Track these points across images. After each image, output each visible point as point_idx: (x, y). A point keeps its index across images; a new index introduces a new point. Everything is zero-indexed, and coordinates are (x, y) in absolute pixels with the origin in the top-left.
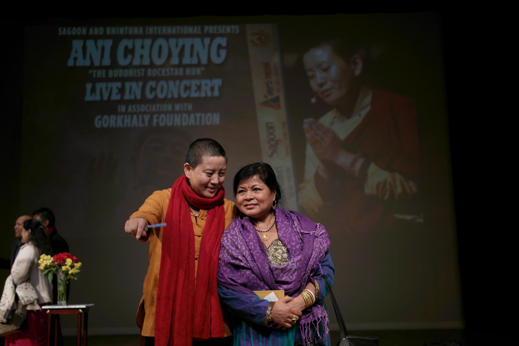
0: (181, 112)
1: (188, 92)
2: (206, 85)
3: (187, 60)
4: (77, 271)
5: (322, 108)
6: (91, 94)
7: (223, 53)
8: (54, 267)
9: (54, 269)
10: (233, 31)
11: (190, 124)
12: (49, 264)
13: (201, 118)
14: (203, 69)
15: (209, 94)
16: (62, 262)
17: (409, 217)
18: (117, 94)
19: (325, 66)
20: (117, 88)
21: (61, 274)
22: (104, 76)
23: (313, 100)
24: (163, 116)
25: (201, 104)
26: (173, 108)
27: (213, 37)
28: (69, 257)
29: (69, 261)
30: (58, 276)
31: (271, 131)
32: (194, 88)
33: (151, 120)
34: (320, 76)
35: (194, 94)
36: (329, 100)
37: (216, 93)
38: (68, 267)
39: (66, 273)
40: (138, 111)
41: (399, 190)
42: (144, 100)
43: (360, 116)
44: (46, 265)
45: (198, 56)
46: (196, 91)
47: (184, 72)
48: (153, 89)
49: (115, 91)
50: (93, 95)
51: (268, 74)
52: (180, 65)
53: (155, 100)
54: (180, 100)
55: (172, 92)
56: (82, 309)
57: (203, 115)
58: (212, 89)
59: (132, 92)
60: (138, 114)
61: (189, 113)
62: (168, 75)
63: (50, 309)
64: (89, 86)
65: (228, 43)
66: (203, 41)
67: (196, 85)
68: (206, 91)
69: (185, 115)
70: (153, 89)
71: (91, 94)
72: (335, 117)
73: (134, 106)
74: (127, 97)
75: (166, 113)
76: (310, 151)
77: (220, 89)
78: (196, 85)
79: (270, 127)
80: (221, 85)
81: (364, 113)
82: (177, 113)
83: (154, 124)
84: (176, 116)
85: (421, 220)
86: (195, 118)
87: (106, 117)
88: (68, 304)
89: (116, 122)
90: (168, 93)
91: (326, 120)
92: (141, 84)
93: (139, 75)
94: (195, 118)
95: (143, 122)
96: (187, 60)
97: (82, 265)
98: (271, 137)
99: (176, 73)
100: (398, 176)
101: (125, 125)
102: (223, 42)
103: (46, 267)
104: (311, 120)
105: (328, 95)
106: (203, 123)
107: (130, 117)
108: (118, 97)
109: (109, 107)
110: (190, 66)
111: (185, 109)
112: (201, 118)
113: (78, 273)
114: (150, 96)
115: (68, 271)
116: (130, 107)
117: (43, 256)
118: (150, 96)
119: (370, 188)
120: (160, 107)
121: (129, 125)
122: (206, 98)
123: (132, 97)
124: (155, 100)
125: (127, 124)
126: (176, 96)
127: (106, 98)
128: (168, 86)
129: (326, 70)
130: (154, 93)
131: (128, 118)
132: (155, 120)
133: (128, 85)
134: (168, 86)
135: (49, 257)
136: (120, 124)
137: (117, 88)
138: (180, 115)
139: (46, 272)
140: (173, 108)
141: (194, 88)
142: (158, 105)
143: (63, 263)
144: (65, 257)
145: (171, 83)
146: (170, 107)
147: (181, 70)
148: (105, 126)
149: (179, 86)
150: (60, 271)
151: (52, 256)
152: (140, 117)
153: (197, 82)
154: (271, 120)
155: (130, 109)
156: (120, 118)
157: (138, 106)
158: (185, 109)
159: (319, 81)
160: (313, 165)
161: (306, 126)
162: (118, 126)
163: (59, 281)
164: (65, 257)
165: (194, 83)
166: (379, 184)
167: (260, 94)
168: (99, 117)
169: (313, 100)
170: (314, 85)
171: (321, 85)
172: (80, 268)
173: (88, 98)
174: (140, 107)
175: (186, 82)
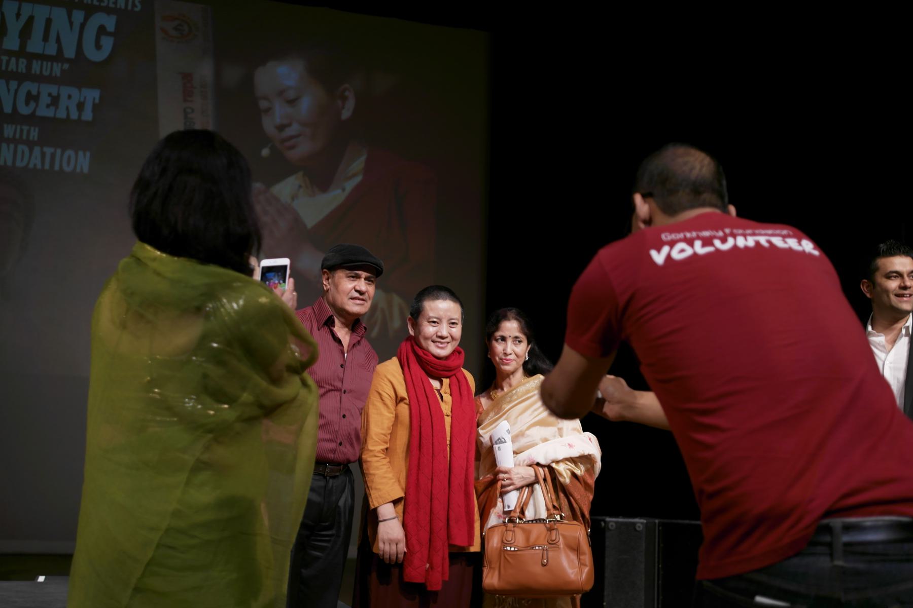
1: (32, 105)
2: (70, 97)
3: (35, 45)
7: (108, 43)
10: (130, 7)
11: (31, 166)
13: (53, 156)
14: (66, 66)
15: (74, 115)
19: (291, 94)
23: (265, 152)
25: (55, 132)
27: (90, 11)
32: (45, 100)
34: (280, 112)
35: (43, 111)
36: (293, 155)
37: (88, 115)
43: (344, 190)
45: (58, 40)
46: (48, 106)
47: (29, 67)
51: (187, 94)
52: (22, 53)
57: (59, 151)
58: (80, 106)
61: (31, 145)
65: (118, 25)
66: (70, 16)
67: (50, 95)
68: (67, 108)
69: (21, 147)
72: (300, 187)
77: (95, 106)
78: (50, 95)
80: (97, 101)
81: (350, 186)
86: (43, 155)
91: (285, 189)
94: (43, 155)
96: (35, 45)
99: (12, 66)
100: (397, 300)
102: (110, 23)
105: (292, 147)
106: (57, 168)
110: (42, 57)
111: (24, 137)
112: (53, 156)
129: (292, 102)
138: (12, 146)
141: (45, 100)
147: (23, 62)
149: (16, 91)
158: (24, 137)
159: (278, 121)
165: (47, 90)
169: (265, 152)
170: (269, 124)
171: (281, 128)
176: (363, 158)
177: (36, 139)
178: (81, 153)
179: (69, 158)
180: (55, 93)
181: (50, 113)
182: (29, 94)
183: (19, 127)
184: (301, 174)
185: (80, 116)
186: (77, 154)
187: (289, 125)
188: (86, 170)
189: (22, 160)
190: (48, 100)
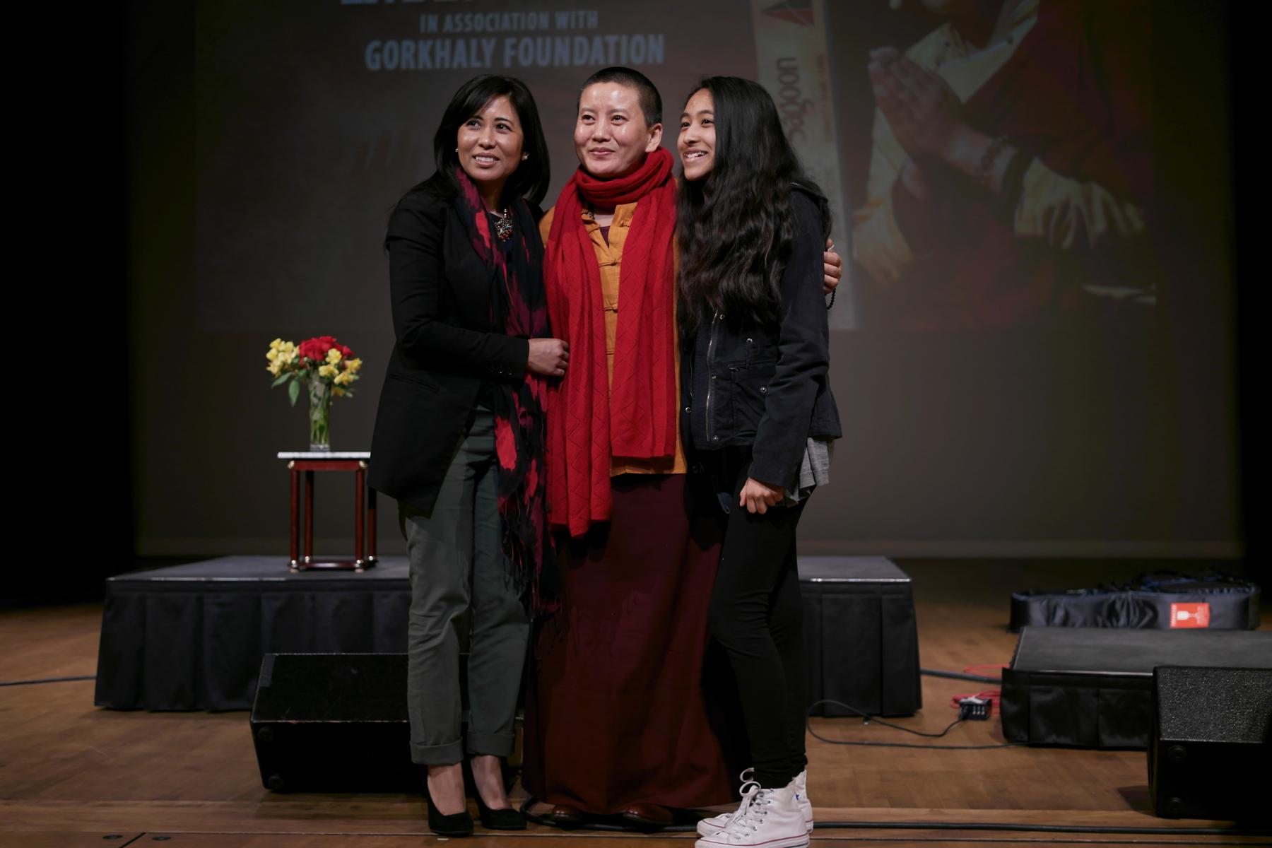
0: (571, 32)
4: (352, 377)
5: (916, 23)
8: (302, 367)
9: (302, 373)
11: (592, 62)
12: (289, 361)
13: (618, 45)
16: (318, 357)
17: (1120, 293)
21: (316, 383)
24: (527, 41)
26: (552, 21)
28: (333, 346)
29: (334, 355)
30: (311, 388)
33: (499, 50)
38: (331, 367)
39: (328, 382)
40: (468, 29)
41: (1100, 226)
43: (1010, 41)
44: (284, 364)
56: (365, 460)
57: (624, 38)
60: (466, 36)
61: (589, 34)
69: (580, 40)
72: (947, 45)
73: (458, 17)
75: (534, 34)
76: (882, 128)
79: (786, 70)
81: (1019, 34)
83: (507, 63)
84: (558, 40)
85: (1152, 300)
86: (606, 46)
87: (392, 44)
88: (332, 450)
89: (416, 56)
91: (925, 51)
94: (606, 46)
95: (480, 56)
97: (362, 366)
98: (789, 93)
100: (1098, 192)
101: (438, 65)
103: (284, 369)
104: (888, 50)
107: (448, 43)
111: (581, 25)
112: (618, 45)
113: (355, 381)
115: (332, 376)
116: (448, 18)
117: (276, 344)
119: (1028, 219)
120: (519, 19)
121: (447, 65)
125: (443, 60)
131: (443, 47)
132: (508, 53)
135: (290, 344)
136: (424, 61)
138: (567, 40)
139: (283, 379)
140: (552, 21)
142: (515, 15)
143: (322, 359)
144: (325, 346)
148: (391, 66)
150: (314, 376)
151: (295, 345)
152: (474, 42)
155: (448, 26)
156: (424, 47)
157: (468, 16)
158: (581, 25)
160: (889, 163)
161: (873, 67)
162: (421, 67)
163: (314, 400)
164: (325, 346)
166: (1050, 210)
168: (375, 44)
172: (358, 372)
174: (472, 20)
188: (660, 59)
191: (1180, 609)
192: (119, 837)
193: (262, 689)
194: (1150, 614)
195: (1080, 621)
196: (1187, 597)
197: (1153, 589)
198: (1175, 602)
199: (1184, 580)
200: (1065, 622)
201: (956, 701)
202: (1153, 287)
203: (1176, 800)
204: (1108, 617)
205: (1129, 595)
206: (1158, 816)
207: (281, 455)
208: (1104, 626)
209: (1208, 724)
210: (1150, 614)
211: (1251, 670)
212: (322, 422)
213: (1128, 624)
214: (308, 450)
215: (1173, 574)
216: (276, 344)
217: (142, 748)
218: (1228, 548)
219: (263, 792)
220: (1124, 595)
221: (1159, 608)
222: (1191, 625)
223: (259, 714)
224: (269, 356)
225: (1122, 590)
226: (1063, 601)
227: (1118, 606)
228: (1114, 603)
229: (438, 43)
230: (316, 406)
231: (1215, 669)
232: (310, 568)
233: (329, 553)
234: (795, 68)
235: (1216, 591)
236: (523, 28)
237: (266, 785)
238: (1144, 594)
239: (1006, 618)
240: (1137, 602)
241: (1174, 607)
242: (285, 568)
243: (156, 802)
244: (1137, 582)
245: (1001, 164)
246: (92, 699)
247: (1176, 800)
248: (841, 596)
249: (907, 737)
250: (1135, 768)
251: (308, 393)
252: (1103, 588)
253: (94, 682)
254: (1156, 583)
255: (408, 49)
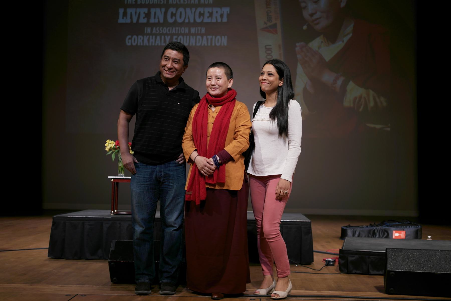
0: (196, 35)
1: (202, 17)
2: (217, 12)
5: (312, 34)
6: (123, 18)
9: (116, 151)
11: (203, 45)
13: (212, 39)
15: (219, 20)
17: (378, 126)
18: (144, 18)
20: (144, 13)
22: (134, 3)
23: (305, 27)
25: (213, 29)
26: (190, 31)
30: (119, 156)
31: (269, 52)
32: (207, 15)
34: (311, 7)
35: (206, 20)
36: (318, 27)
37: (225, 20)
40: (161, 32)
41: (372, 104)
42: (165, 24)
43: (343, 42)
44: (110, 147)
46: (208, 17)
48: (173, 15)
49: (142, 15)
50: (125, 18)
53: (175, 24)
54: (195, 24)
55: (189, 18)
57: (214, 37)
58: (222, 16)
59: (157, 17)
60: (161, 35)
61: (202, 35)
62: (185, 3)
63: (113, 179)
64: (121, 11)
67: (209, 12)
68: (216, 18)
69: (199, 37)
70: (173, 15)
71: (123, 18)
72: (322, 42)
73: (158, 28)
74: (152, 21)
75: (183, 35)
76: (300, 69)
77: (228, 15)
78: (209, 12)
80: (228, 13)
81: (346, 39)
82: (193, 35)
84: (191, 37)
85: (389, 129)
86: (207, 39)
87: (135, 37)
88: (125, 176)
89: (143, 41)
90: (185, 18)
91: (315, 44)
92: (163, 10)
93: (162, 3)
94: (207, 39)
100: (371, 92)
101: (150, 44)
103: (110, 149)
104: (302, 43)
105: (317, 24)
106: (213, 45)
107: (154, 37)
108: (145, 21)
109: (137, 29)
111: (199, 32)
112: (212, 39)
114: (170, 20)
116: (154, 29)
118: (170, 20)
119: (348, 101)
120: (178, 30)
121: (153, 44)
122: (217, 23)
123: (156, 21)
124: (175, 24)
125: (152, 42)
126: (192, 21)
127: (135, 21)
128: (186, 12)
130: (174, 18)
131: (152, 38)
133: (153, 11)
134: (186, 12)
135: (113, 141)
137: (144, 13)
138: (194, 37)
139: (110, 152)
140: (190, 31)
141: (207, 15)
142: (177, 28)
145: (188, 10)
146: (187, 30)
148: (134, 44)
149: (195, 12)
152: (163, 37)
153: (210, 10)
154: (270, 43)
155: (154, 31)
156: (146, 38)
157: (161, 28)
158: (199, 32)
161: (297, 49)
162: (145, 44)
165: (207, 10)
166: (355, 98)
167: (261, 21)
168: (130, 36)
169: (305, 27)
170: (306, 14)
171: (312, 15)
173: (121, 20)
174: (162, 29)
175: (200, 10)
176: (352, 25)
177: (204, 32)
178: (223, 37)
179: (218, 40)
180: (211, 11)
181: (209, 20)
182: (200, 13)
183: (197, 28)
184: (322, 36)
185: (222, 20)
186: (221, 37)
187: (315, 13)
188: (226, 44)
189: (199, 43)
190: (208, 15)
191: (396, 233)
192: (70, 295)
193: (112, 251)
194: (386, 234)
195: (364, 235)
196: (398, 229)
197: (388, 226)
198: (395, 230)
199: (397, 223)
200: (359, 236)
201: (324, 260)
202: (389, 125)
203: (392, 289)
204: (373, 234)
205: (380, 228)
206: (387, 294)
207: (109, 177)
208: (371, 237)
209: (402, 266)
210: (386, 234)
211: (415, 249)
212: (122, 167)
213: (379, 237)
214: (118, 176)
215: (394, 221)
216: (108, 141)
217: (67, 270)
218: (413, 213)
219: (111, 283)
220: (378, 228)
221: (389, 232)
222: (399, 238)
223: (111, 259)
224: (106, 145)
225: (377, 226)
226: (358, 230)
227: (376, 231)
228: (375, 230)
229: (151, 37)
230: (120, 162)
231: (404, 249)
232: (117, 214)
233: (124, 210)
234: (271, 49)
235: (408, 227)
236: (179, 32)
237: (112, 281)
238: (384, 227)
239: (339, 234)
240: (382, 230)
241: (394, 232)
242: (109, 214)
243: (78, 286)
244: (382, 224)
245: (339, 82)
246: (47, 255)
247: (392, 289)
248: (289, 226)
249: (310, 270)
250: (380, 281)
251: (118, 157)
252: (371, 226)
253: (48, 250)
254: (388, 224)
255: (140, 38)
